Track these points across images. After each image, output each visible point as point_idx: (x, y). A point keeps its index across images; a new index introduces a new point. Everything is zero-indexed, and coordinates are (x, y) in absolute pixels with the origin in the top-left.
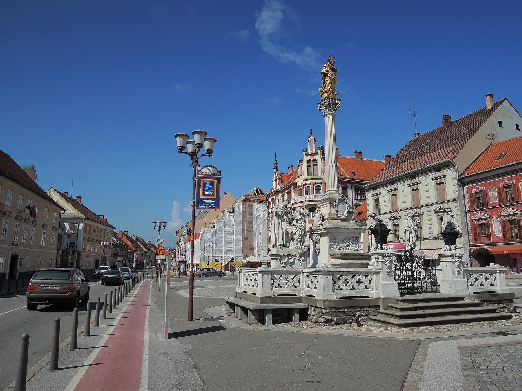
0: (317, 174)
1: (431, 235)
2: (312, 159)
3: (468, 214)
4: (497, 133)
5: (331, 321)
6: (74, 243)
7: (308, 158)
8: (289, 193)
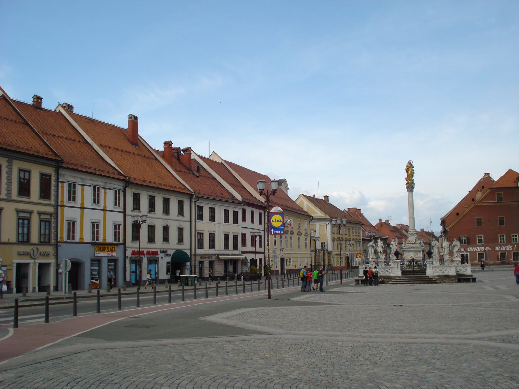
6: (324, 243)
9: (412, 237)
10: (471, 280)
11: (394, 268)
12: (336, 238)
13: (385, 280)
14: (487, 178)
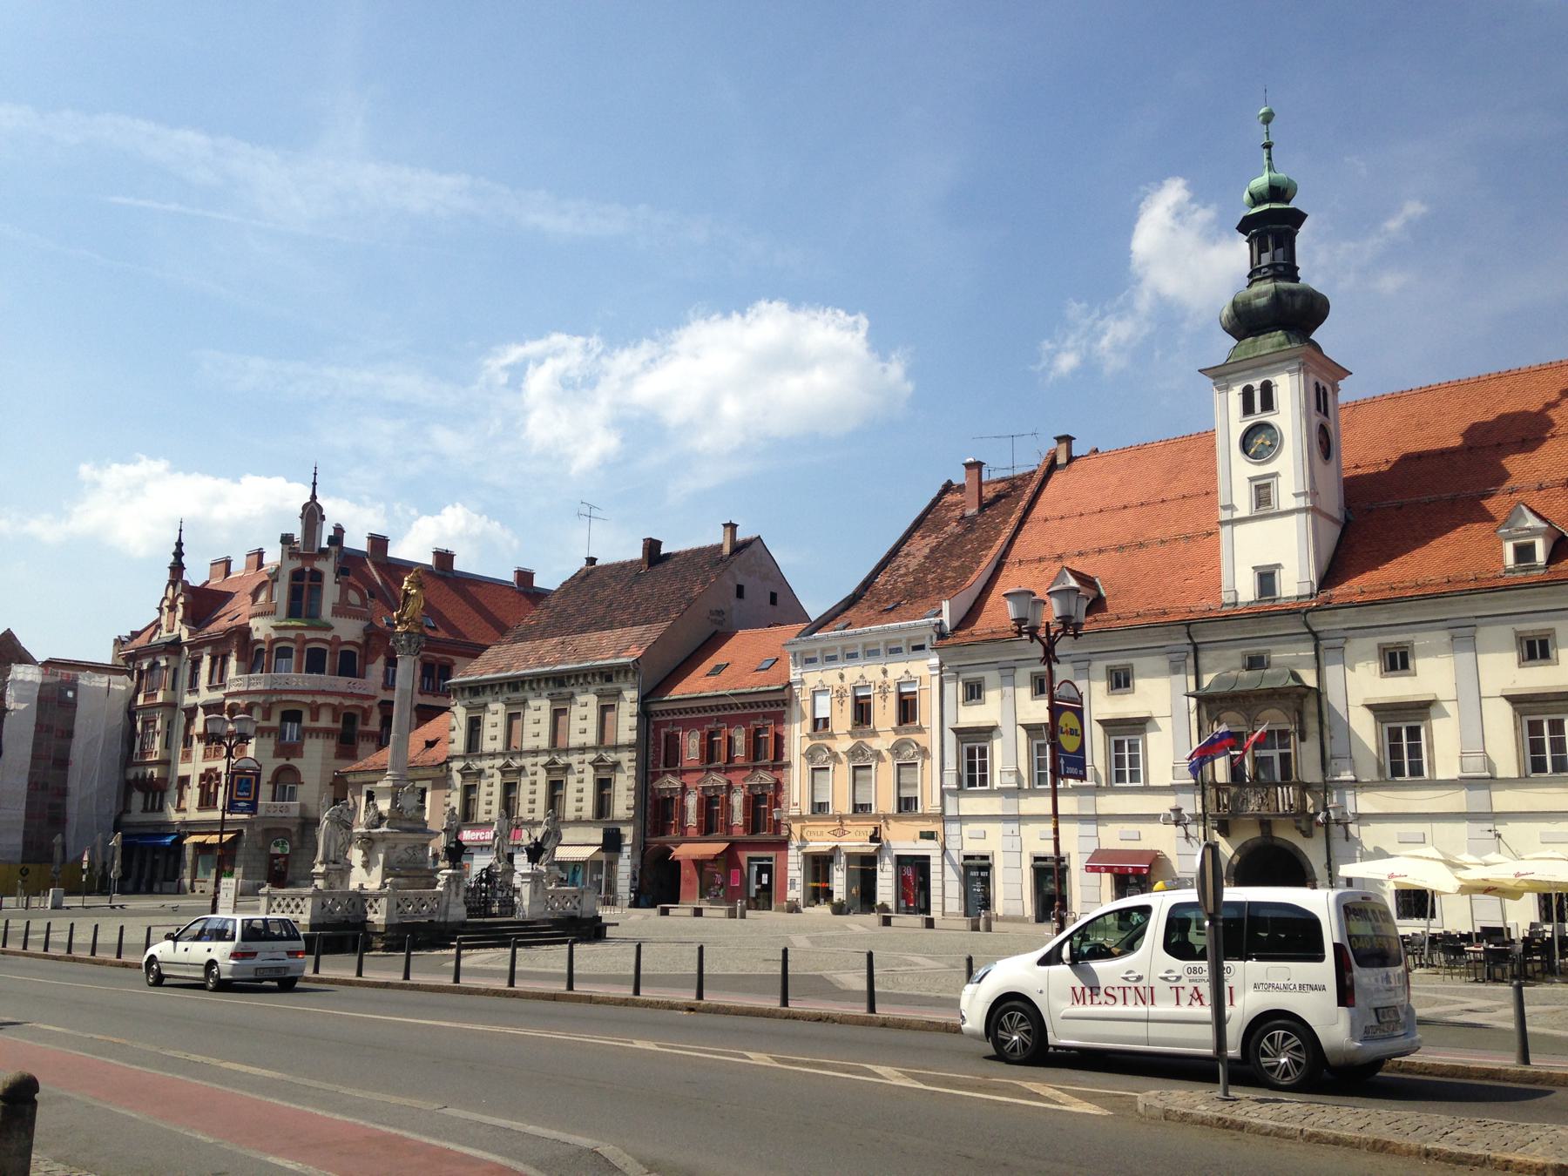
2: (307, 569)
7: (297, 564)
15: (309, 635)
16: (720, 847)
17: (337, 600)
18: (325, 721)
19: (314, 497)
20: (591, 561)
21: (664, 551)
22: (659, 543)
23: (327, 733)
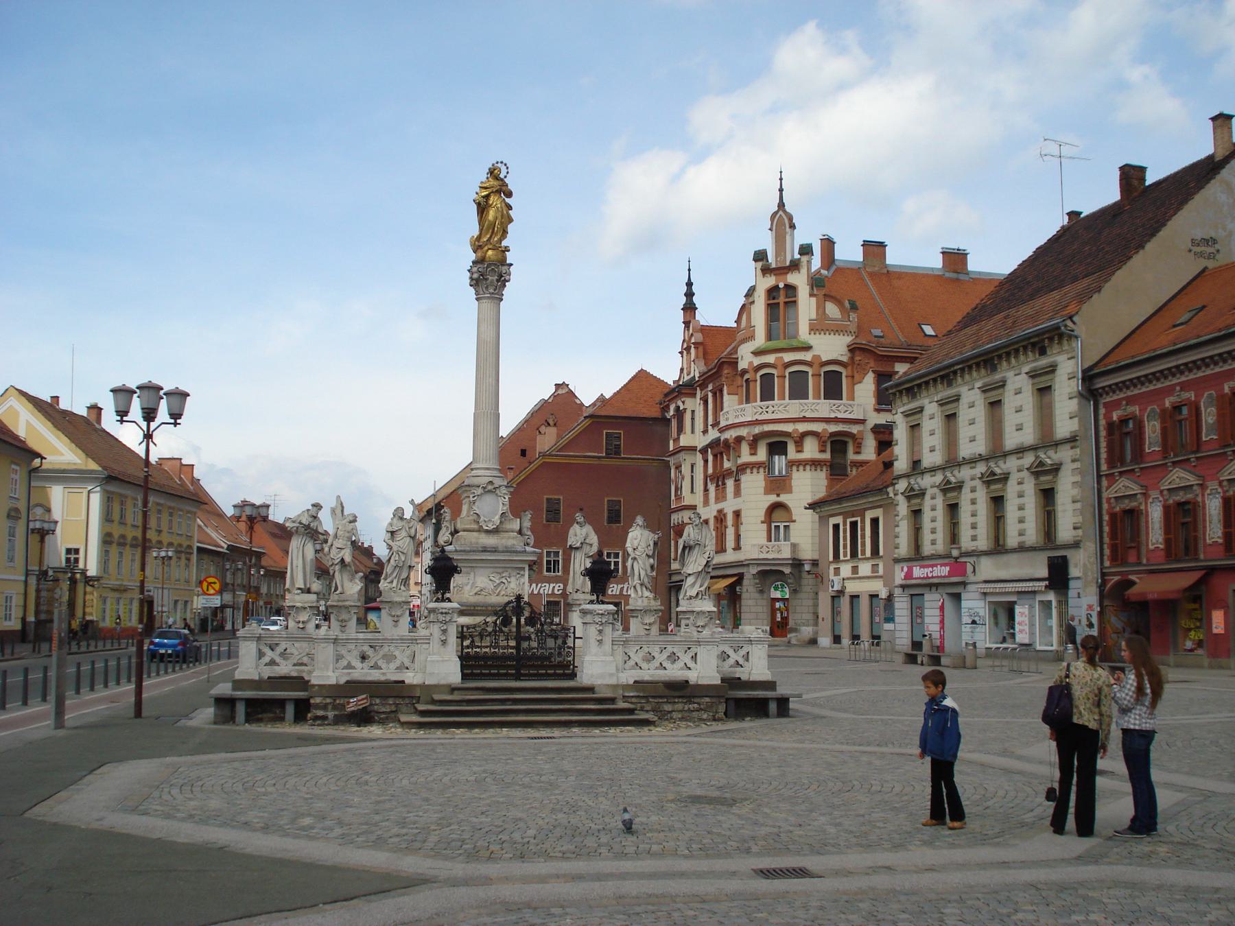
0: (795, 336)
1: (1022, 539)
2: (781, 285)
3: (1105, 483)
4: (1230, 234)
5: (324, 718)
6: (77, 551)
7: (771, 281)
8: (718, 394)
9: (489, 499)
10: (773, 707)
11: (427, 640)
12: (116, 536)
13: (380, 706)
14: (564, 397)
15: (788, 357)
16: (1186, 580)
17: (814, 316)
18: (811, 450)
19: (781, 205)
20: (1073, 215)
21: (1150, 179)
22: (1142, 170)
23: (815, 464)
